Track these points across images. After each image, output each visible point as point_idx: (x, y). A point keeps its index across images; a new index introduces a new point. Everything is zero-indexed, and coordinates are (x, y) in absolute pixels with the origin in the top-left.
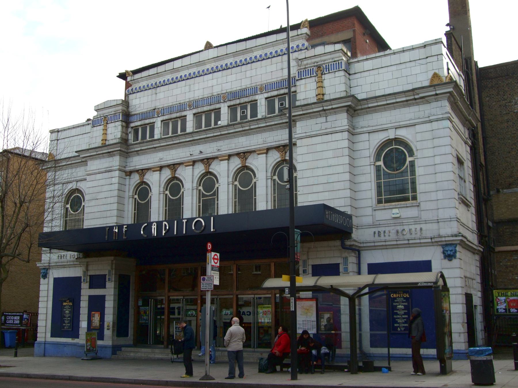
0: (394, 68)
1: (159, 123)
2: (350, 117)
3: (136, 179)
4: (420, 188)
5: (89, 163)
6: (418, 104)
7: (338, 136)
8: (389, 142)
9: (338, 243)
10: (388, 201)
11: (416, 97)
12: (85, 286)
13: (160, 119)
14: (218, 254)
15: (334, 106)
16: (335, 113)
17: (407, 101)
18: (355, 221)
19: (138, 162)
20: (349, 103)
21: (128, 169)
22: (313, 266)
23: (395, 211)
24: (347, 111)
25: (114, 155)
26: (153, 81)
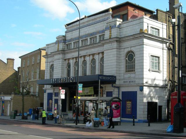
0: (131, 26)
1: (73, 43)
2: (118, 43)
3: (67, 61)
4: (136, 67)
5: (55, 56)
6: (136, 39)
7: (114, 50)
8: (129, 52)
9: (111, 85)
10: (129, 71)
11: (135, 37)
12: (53, 96)
13: (73, 42)
14: (64, 90)
15: (112, 40)
16: (113, 42)
17: (133, 38)
18: (117, 78)
19: (69, 56)
20: (116, 40)
21: (65, 58)
22: (107, 92)
23: (129, 75)
24: (117, 42)
25: (60, 54)
26: (72, 29)
